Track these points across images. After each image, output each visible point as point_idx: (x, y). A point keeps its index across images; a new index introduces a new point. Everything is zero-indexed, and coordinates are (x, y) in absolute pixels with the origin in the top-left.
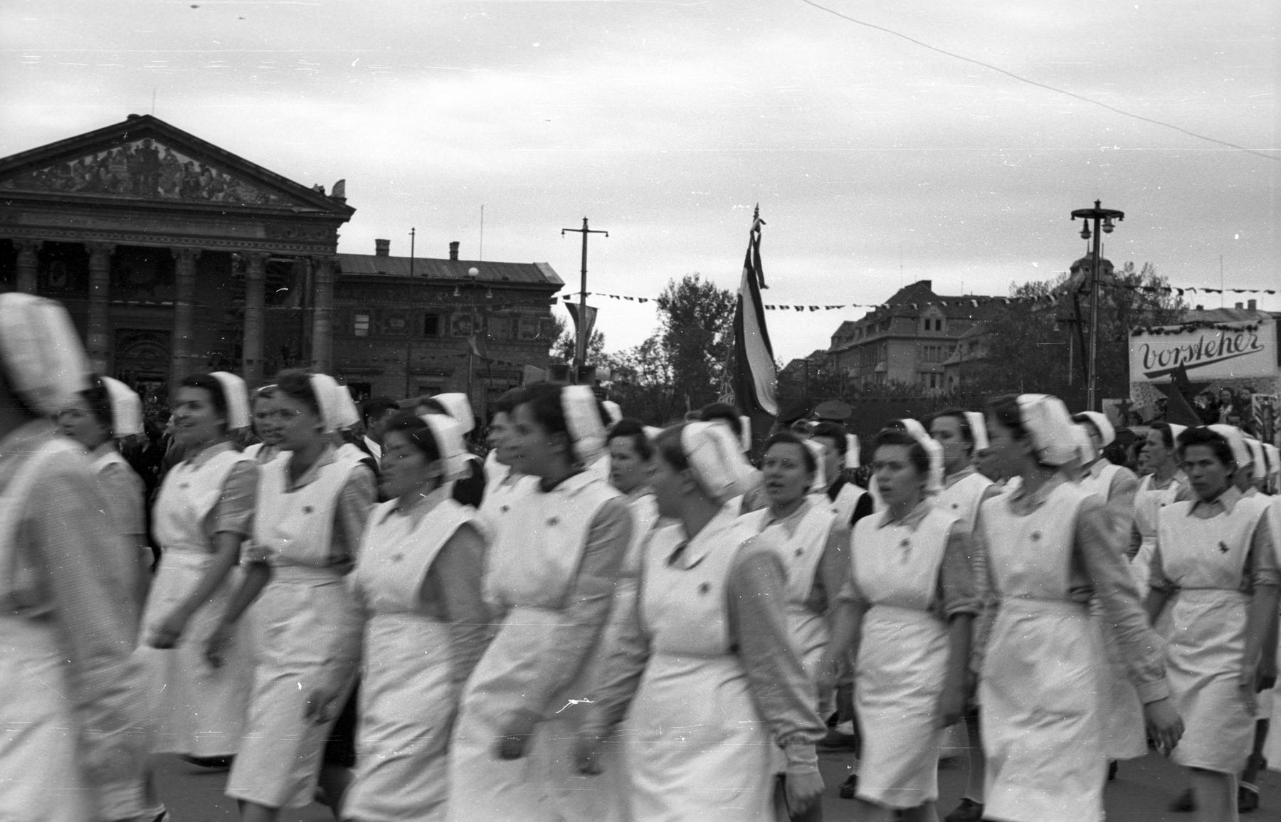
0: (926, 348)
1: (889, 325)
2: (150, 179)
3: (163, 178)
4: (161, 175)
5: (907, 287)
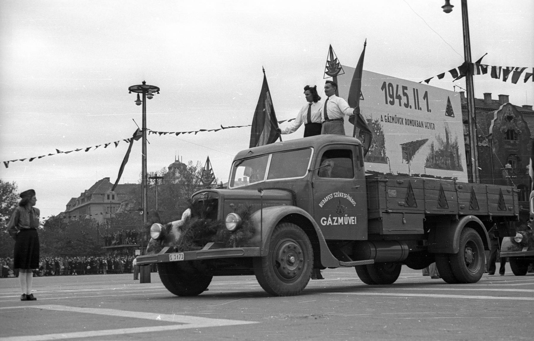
0: (108, 207)
1: (91, 198)
5: (99, 181)
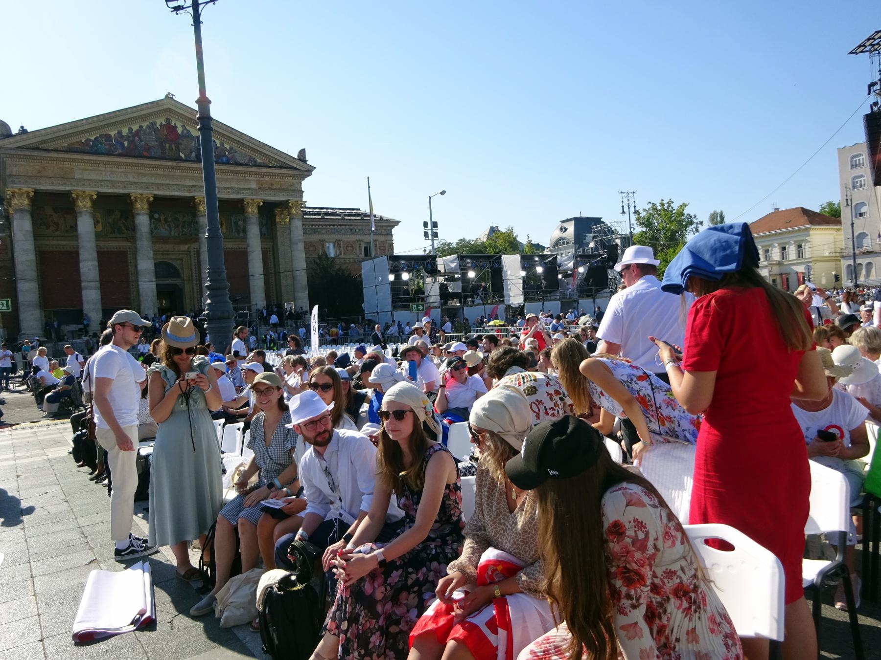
2: (173, 147)
3: (182, 146)
4: (181, 144)
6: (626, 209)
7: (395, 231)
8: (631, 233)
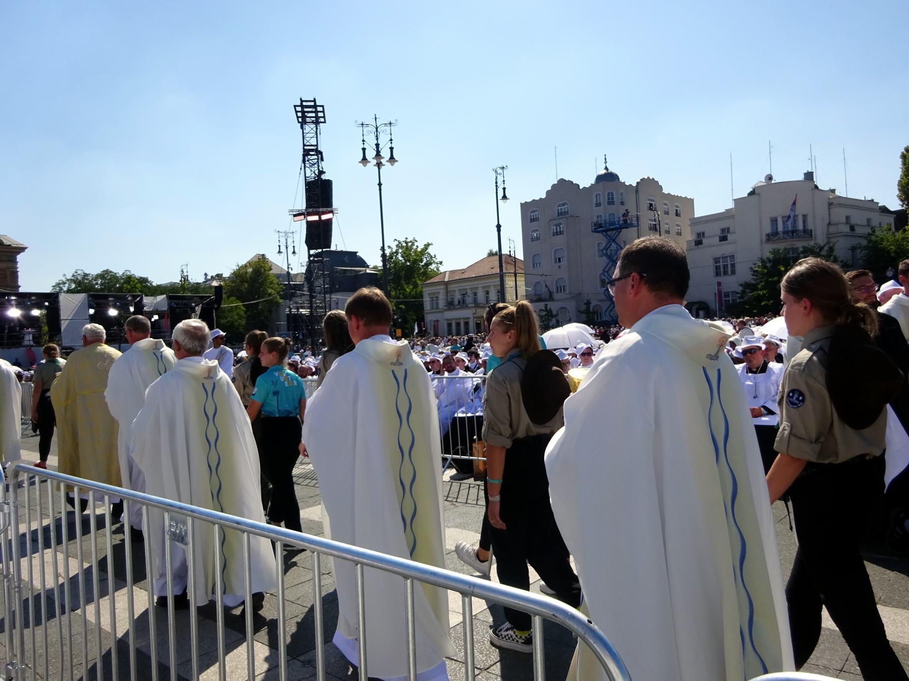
6: (283, 249)
7: (20, 258)
8: (288, 273)
